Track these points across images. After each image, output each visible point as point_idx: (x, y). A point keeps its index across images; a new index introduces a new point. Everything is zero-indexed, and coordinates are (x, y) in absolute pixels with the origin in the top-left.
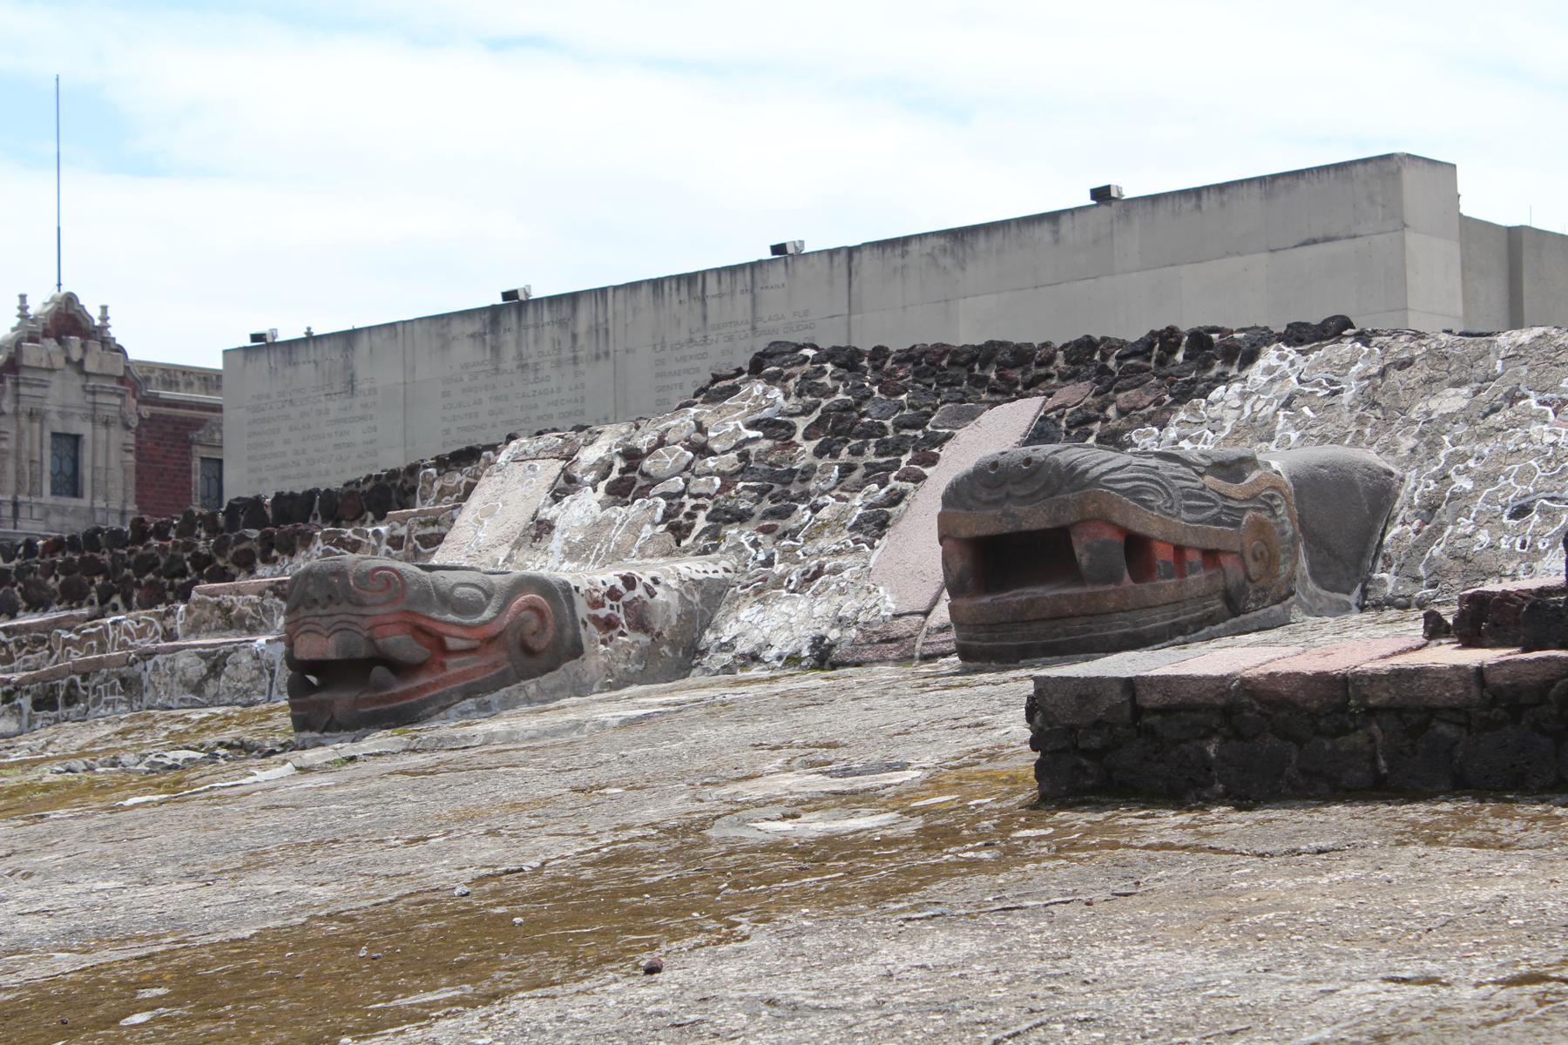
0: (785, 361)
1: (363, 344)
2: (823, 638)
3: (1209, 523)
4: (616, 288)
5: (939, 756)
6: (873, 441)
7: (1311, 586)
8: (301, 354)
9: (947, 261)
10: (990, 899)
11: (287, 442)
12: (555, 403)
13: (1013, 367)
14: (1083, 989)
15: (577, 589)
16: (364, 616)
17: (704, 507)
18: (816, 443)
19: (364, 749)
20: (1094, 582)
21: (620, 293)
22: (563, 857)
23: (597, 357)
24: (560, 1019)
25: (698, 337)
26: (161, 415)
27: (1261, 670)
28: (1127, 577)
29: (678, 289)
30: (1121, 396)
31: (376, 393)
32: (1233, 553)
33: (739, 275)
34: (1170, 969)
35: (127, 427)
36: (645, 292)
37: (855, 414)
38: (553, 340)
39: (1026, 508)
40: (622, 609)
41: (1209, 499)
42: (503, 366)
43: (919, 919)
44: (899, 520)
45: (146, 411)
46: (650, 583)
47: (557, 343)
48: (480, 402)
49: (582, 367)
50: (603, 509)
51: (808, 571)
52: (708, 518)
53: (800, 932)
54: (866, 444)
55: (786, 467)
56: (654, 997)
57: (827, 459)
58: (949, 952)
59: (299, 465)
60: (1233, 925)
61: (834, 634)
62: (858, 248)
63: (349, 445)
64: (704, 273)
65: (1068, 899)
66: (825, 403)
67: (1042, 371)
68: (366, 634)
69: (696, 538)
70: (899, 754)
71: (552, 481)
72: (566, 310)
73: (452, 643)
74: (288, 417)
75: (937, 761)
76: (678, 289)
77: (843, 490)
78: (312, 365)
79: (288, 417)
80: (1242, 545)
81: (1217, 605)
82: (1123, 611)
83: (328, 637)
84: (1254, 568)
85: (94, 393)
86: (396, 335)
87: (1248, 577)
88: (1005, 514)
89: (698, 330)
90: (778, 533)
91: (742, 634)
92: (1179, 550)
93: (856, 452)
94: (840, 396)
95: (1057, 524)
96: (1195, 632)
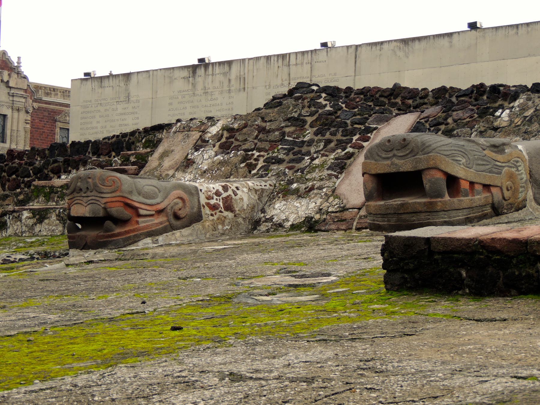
0: (304, 91)
1: (134, 79)
2: (312, 218)
3: (486, 172)
4: (249, 59)
5: (346, 271)
6: (341, 129)
7: (533, 203)
8: (106, 83)
9: (401, 54)
10: (347, 334)
11: (98, 122)
12: (219, 110)
13: (408, 99)
14: (374, 375)
15: (201, 190)
16: (102, 197)
17: (263, 156)
18: (315, 129)
19: (98, 258)
20: (431, 197)
21: (251, 61)
22: (165, 307)
23: (240, 90)
24: (135, 377)
26: (43, 108)
27: (489, 237)
28: (447, 195)
29: (278, 61)
30: (455, 113)
32: (497, 186)
34: (417, 368)
35: (27, 112)
36: (263, 61)
37: (334, 117)
39: (402, 161)
40: (221, 200)
41: (488, 161)
43: (312, 341)
44: (350, 165)
45: (36, 105)
46: (235, 189)
47: (221, 83)
48: (186, 108)
49: (232, 94)
50: (216, 155)
51: (308, 187)
52: (264, 161)
53: (256, 344)
54: (337, 131)
55: (300, 140)
56: (180, 369)
57: (319, 137)
58: (320, 356)
60: (453, 350)
61: (317, 217)
62: (360, 45)
63: (126, 125)
64: (290, 54)
65: (383, 335)
66: (320, 111)
67: (422, 101)
68: (103, 206)
69: (258, 170)
70: (330, 269)
71: (195, 141)
73: (142, 212)
74: (99, 111)
75: (345, 273)
76: (278, 61)
77: (325, 151)
78: (111, 88)
79: (99, 111)
80: (502, 183)
81: (488, 210)
82: (444, 211)
83: (86, 207)
84: (507, 194)
85: (13, 96)
87: (504, 198)
88: (392, 164)
90: (295, 169)
91: (276, 215)
92: (472, 184)
93: (333, 134)
94: (328, 108)
95: (415, 169)
96: (478, 222)
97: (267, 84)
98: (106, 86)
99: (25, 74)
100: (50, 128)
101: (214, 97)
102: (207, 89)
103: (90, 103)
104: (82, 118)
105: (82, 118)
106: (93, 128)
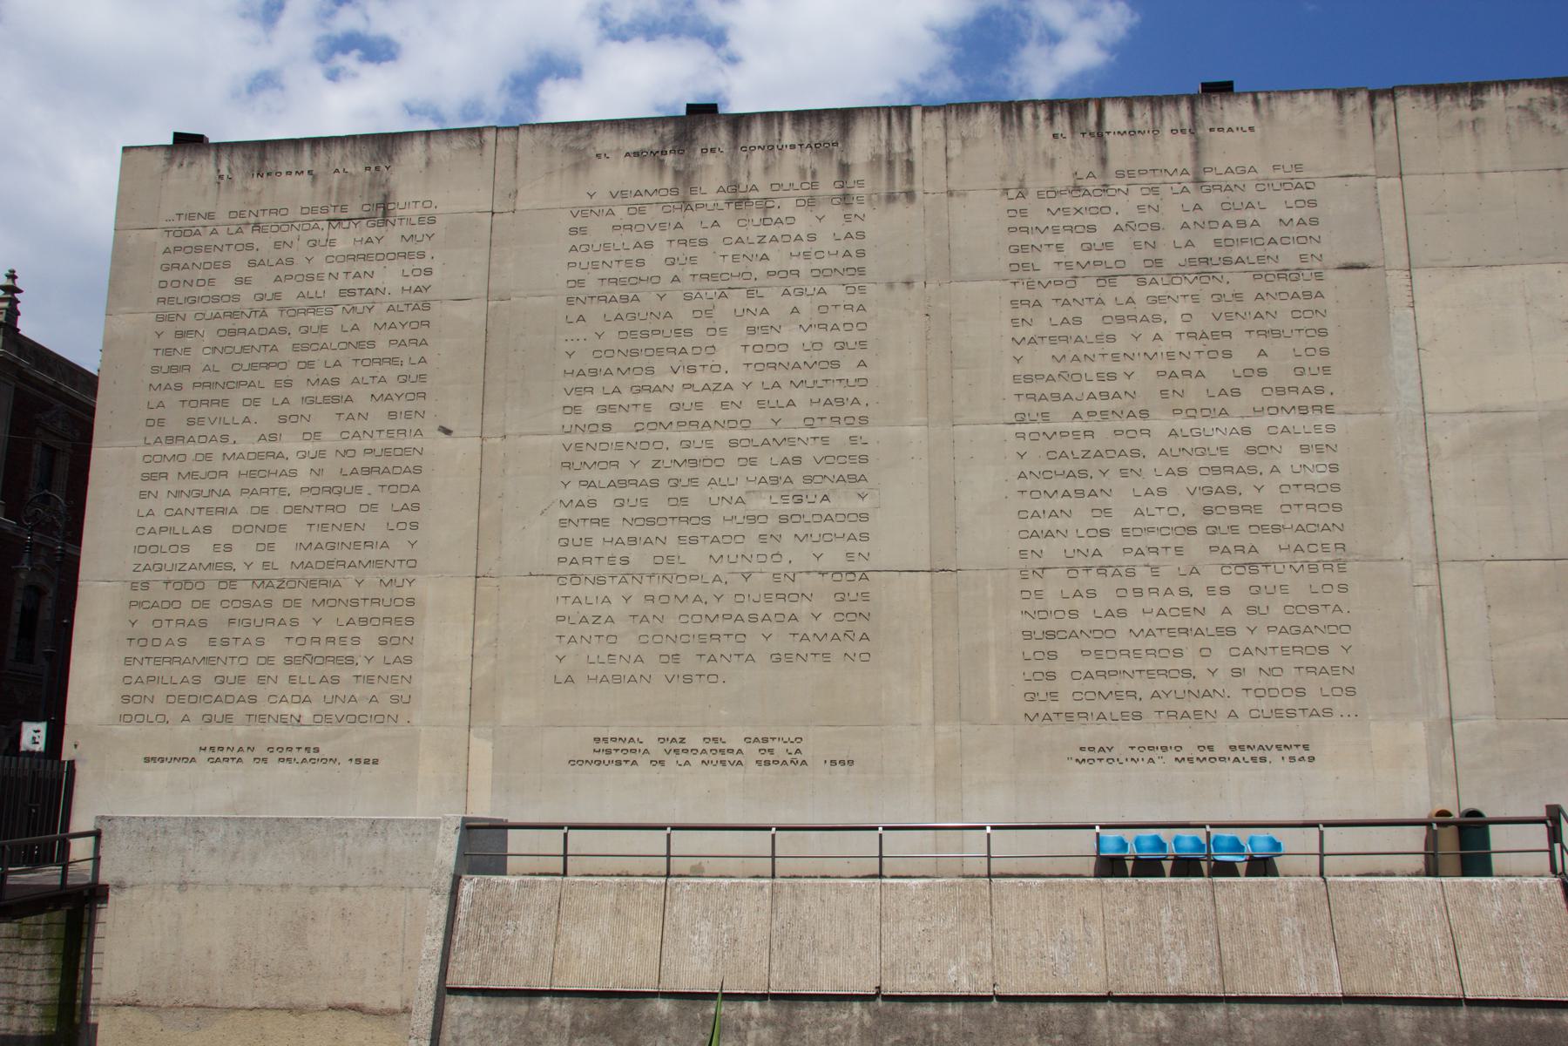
1: (414, 154)
11: (241, 281)
12: (806, 255)
23: (891, 198)
25: (1090, 184)
31: (432, 220)
33: (1168, 110)
38: (802, 171)
42: (696, 199)
47: (810, 177)
49: (857, 208)
59: (264, 314)
72: (828, 132)
74: (249, 246)
76: (1051, 118)
86: (482, 145)
89: (1091, 175)
97: (1014, 183)
101: (773, 214)
102: (742, 188)
103: (206, 222)
104: (167, 268)
105: (167, 268)
106: (216, 299)
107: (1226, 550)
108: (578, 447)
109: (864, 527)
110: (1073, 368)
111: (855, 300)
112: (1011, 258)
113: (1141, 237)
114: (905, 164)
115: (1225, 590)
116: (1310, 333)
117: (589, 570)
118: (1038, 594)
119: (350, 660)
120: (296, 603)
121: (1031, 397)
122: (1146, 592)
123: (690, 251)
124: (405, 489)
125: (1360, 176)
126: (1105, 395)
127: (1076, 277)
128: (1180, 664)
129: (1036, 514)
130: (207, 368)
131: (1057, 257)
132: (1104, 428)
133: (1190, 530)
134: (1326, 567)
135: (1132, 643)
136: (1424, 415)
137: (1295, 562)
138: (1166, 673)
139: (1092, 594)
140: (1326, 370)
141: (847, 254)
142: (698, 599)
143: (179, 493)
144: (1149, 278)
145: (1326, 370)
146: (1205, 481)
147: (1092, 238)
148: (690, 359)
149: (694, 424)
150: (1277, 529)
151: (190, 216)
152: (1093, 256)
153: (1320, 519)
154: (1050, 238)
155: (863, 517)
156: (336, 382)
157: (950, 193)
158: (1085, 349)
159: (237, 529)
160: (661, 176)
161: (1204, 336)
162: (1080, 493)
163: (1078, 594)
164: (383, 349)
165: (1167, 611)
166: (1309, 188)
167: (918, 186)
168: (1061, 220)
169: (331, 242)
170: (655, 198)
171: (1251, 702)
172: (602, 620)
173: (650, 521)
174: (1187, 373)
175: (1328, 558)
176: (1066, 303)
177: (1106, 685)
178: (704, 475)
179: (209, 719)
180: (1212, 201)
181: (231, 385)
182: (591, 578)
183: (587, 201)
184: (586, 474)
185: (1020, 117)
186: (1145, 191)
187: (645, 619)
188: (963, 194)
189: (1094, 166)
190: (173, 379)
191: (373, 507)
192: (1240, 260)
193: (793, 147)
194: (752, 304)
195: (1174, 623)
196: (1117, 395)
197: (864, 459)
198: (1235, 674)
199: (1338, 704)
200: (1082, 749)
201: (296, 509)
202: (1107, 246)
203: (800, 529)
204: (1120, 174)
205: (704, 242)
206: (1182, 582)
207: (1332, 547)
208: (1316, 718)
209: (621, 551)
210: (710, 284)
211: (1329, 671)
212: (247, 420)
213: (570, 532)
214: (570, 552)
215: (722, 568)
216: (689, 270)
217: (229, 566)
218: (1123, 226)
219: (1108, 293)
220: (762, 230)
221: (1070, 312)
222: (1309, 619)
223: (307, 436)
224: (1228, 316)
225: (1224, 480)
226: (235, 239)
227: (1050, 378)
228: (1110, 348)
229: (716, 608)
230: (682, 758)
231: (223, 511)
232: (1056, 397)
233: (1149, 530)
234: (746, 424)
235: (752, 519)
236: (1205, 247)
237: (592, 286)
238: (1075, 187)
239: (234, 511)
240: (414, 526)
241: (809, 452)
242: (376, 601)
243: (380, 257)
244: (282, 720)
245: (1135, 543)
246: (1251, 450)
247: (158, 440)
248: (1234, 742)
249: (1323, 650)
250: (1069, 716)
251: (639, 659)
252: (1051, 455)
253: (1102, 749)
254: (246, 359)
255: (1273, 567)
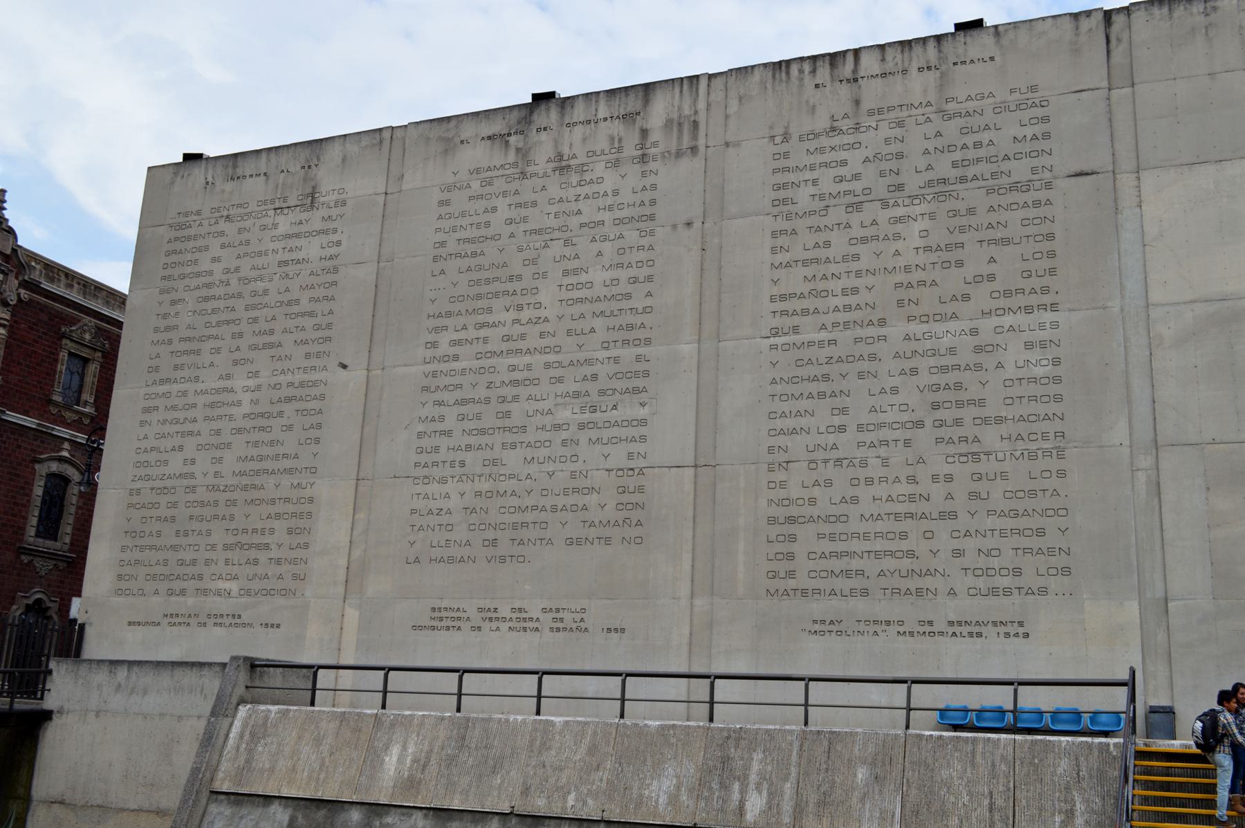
4: (711, 77)
8: (247, 168)
11: (215, 260)
12: (610, 208)
23: (679, 154)
25: (844, 125)
26: (38, 303)
31: (344, 203)
38: (612, 138)
48: (495, 209)
49: (652, 166)
59: (228, 284)
64: (857, 52)
72: (633, 103)
74: (222, 233)
76: (814, 71)
78: (263, 178)
86: (381, 142)
89: (846, 116)
97: (779, 131)
98: (247, 174)
99: (10, 224)
100: (49, 346)
102: (565, 157)
103: (195, 218)
104: (168, 254)
106: (198, 275)
107: (951, 441)
108: (434, 374)
109: (643, 430)
110: (821, 285)
111: (645, 242)
112: (774, 195)
113: (886, 166)
114: (692, 124)
115: (949, 478)
116: (1037, 238)
117: (436, 472)
118: (783, 485)
119: (267, 547)
120: (234, 503)
121: (784, 313)
122: (876, 481)
123: (524, 212)
124: (313, 412)
125: (1092, 90)
126: (848, 308)
127: (828, 206)
128: (904, 545)
129: (783, 415)
130: (189, 327)
131: (811, 190)
132: (845, 337)
133: (919, 424)
134: (1045, 454)
135: (862, 527)
136: (1148, 307)
137: (1016, 450)
138: (892, 554)
139: (829, 483)
140: (1052, 272)
141: (642, 204)
142: (514, 493)
143: (165, 421)
144: (891, 202)
145: (1052, 272)
146: (935, 379)
147: (842, 171)
148: (519, 300)
149: (518, 351)
150: (1000, 420)
151: (186, 214)
152: (845, 186)
153: (1041, 409)
154: (808, 175)
155: (643, 422)
156: (272, 332)
157: (727, 144)
158: (833, 268)
159: (200, 447)
160: (506, 155)
161: (939, 248)
162: (822, 395)
163: (816, 484)
164: (305, 305)
165: (894, 497)
166: (1043, 106)
167: (701, 142)
168: (820, 159)
169: (275, 226)
170: (501, 172)
171: (970, 580)
172: (443, 513)
173: (482, 432)
174: (922, 283)
175: (1047, 445)
176: (819, 229)
177: (837, 565)
178: (523, 392)
179: (171, 593)
180: (951, 128)
181: (203, 339)
182: (437, 478)
183: (451, 179)
184: (439, 396)
185: (788, 73)
186: (892, 125)
187: (474, 511)
188: (737, 144)
189: (848, 108)
190: (165, 336)
191: (290, 428)
192: (975, 178)
193: (605, 119)
194: (568, 251)
195: (901, 508)
196: (858, 307)
197: (646, 374)
198: (955, 555)
199: (1053, 583)
200: (815, 622)
201: (239, 431)
202: (856, 177)
203: (594, 434)
204: (871, 113)
205: (534, 204)
206: (909, 471)
207: (1052, 436)
208: (1032, 597)
209: (460, 456)
210: (538, 237)
211: (1046, 552)
212: (212, 365)
213: (426, 442)
214: (424, 458)
215: (533, 469)
216: (523, 227)
217: (192, 476)
218: (871, 158)
219: (855, 218)
220: (579, 190)
221: (821, 237)
222: (1029, 504)
223: (250, 375)
224: (962, 230)
225: (951, 378)
226: (213, 229)
227: (802, 296)
228: (854, 266)
229: (529, 501)
230: (494, 625)
231: (191, 433)
232: (805, 312)
233: (881, 425)
234: (557, 350)
235: (557, 427)
236: (944, 168)
237: (452, 247)
238: (832, 128)
239: (199, 434)
240: (317, 441)
241: (603, 370)
242: (287, 500)
243: (307, 234)
244: (218, 593)
245: (869, 437)
246: (978, 349)
247: (154, 383)
248: (952, 617)
249: (1041, 532)
250: (804, 593)
251: (468, 543)
252: (799, 363)
253: (832, 622)
254: (214, 319)
255: (994, 455)
